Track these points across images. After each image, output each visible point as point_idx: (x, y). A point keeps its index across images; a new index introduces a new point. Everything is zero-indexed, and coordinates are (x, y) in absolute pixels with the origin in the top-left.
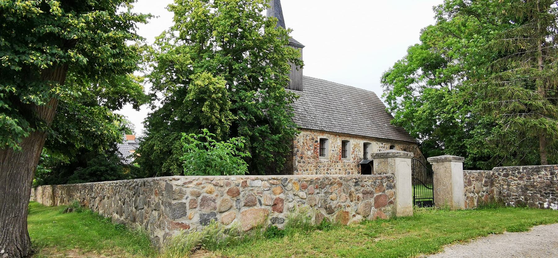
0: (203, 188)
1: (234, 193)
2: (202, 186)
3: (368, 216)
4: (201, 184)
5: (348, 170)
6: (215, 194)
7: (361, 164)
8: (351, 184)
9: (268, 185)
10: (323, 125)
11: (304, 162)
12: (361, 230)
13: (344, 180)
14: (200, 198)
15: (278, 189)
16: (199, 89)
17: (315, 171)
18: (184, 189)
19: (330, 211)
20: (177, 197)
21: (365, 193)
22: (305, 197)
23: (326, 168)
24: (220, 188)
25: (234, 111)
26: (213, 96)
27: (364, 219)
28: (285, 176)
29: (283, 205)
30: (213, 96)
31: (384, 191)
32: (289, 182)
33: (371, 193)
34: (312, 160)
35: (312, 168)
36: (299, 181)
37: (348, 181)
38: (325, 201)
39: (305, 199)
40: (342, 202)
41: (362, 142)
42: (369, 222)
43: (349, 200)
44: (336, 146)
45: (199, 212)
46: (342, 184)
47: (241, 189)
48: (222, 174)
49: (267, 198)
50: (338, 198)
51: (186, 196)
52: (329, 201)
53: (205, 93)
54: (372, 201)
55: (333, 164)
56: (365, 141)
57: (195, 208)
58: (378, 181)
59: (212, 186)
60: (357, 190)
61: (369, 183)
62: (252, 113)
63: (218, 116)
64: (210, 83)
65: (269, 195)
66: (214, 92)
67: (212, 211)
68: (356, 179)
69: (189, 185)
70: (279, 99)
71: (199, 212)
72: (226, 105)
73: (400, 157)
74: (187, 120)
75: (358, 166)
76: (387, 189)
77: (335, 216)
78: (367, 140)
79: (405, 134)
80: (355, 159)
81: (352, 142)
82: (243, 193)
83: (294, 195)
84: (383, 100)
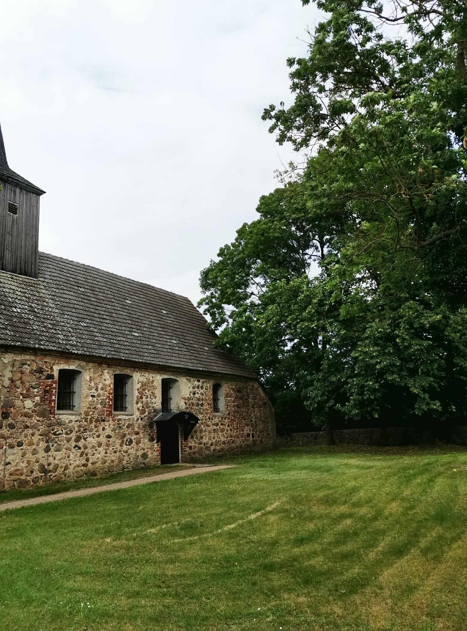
5: (128, 437)
7: (157, 422)
10: (74, 344)
11: (12, 426)
23: (73, 436)
34: (35, 419)
41: (158, 379)
44: (100, 386)
55: (93, 425)
56: (166, 377)
78: (171, 375)
79: (240, 363)
80: (143, 412)
81: (138, 378)
84: (201, 310)
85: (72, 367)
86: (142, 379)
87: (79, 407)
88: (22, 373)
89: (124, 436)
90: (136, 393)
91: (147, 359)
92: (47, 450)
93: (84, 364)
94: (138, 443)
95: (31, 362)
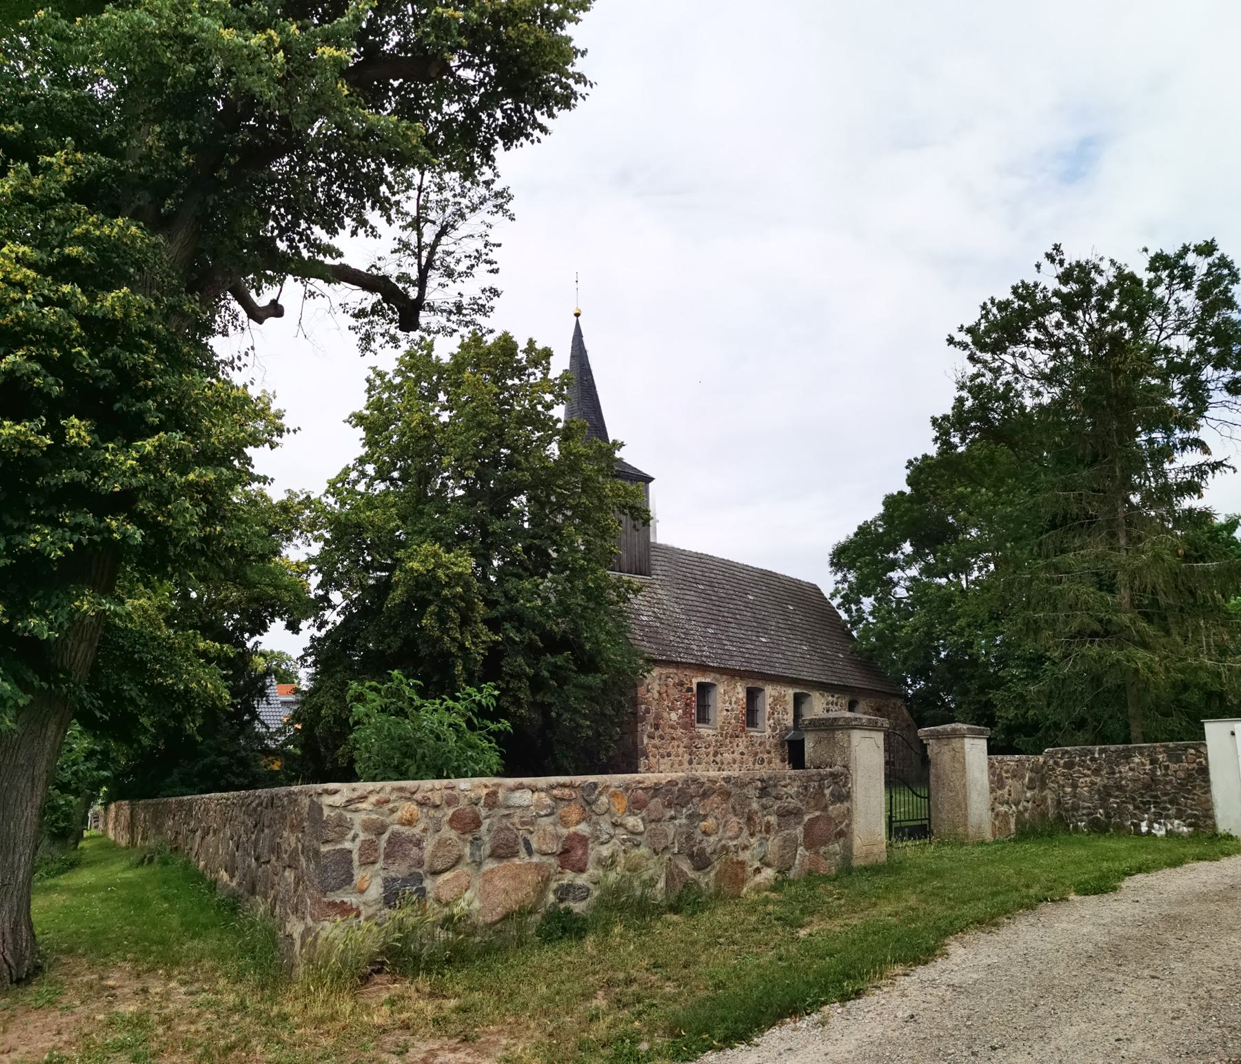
0: (392, 811)
1: (467, 823)
2: (391, 805)
3: (789, 869)
4: (388, 801)
6: (421, 826)
8: (752, 792)
9: (548, 801)
10: (706, 653)
12: (770, 908)
13: (735, 784)
14: (386, 836)
15: (574, 813)
16: (416, 579)
17: (687, 757)
18: (349, 815)
19: (701, 861)
20: (332, 836)
21: (784, 814)
22: (641, 828)
23: (711, 750)
24: (432, 812)
25: (494, 625)
26: (445, 592)
27: (780, 878)
28: (592, 779)
29: (585, 853)
30: (445, 592)
31: (825, 808)
32: (601, 794)
33: (797, 813)
34: (680, 731)
35: (681, 750)
36: (627, 789)
37: (744, 785)
38: (689, 837)
39: (641, 834)
40: (731, 838)
41: (790, 692)
42: (790, 885)
43: (746, 833)
44: (734, 699)
45: (383, 874)
46: (729, 794)
47: (483, 812)
48: (439, 777)
49: (546, 835)
50: (720, 830)
51: (353, 832)
52: (700, 838)
53: (428, 586)
54: (799, 831)
57: (373, 863)
58: (812, 784)
59: (414, 806)
60: (764, 807)
61: (792, 790)
62: (534, 626)
63: (458, 635)
64: (438, 565)
65: (551, 828)
66: (448, 585)
67: (414, 870)
68: (762, 781)
69: (359, 805)
70: (595, 595)
71: (383, 874)
72: (473, 610)
73: (861, 727)
74: (390, 648)
75: (782, 745)
76: (833, 803)
77: (712, 874)
78: (804, 688)
80: (774, 729)
81: (770, 691)
82: (488, 821)
83: (615, 825)
85: (708, 680)
86: (773, 693)
87: (715, 721)
88: (667, 686)
89: (756, 754)
90: (768, 709)
91: (779, 671)
92: (690, 762)
93: (718, 676)
94: (770, 762)
95: (675, 675)
